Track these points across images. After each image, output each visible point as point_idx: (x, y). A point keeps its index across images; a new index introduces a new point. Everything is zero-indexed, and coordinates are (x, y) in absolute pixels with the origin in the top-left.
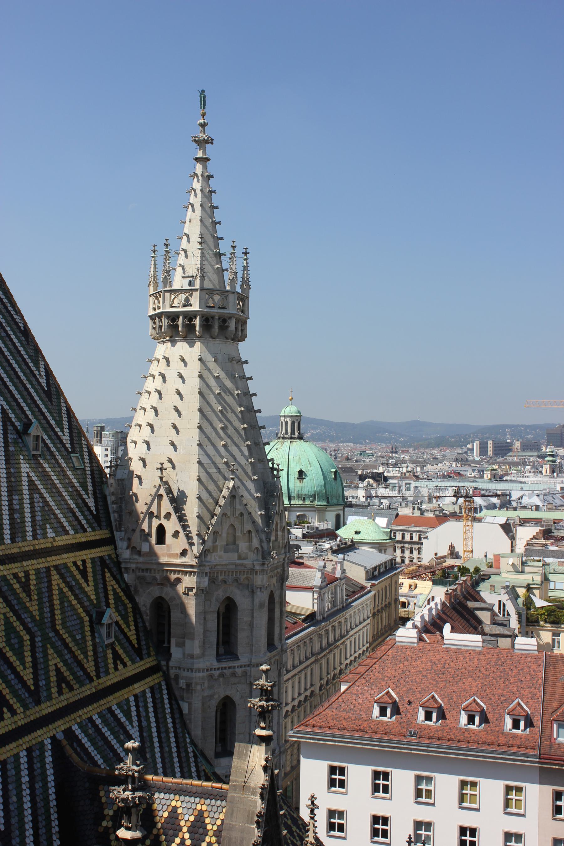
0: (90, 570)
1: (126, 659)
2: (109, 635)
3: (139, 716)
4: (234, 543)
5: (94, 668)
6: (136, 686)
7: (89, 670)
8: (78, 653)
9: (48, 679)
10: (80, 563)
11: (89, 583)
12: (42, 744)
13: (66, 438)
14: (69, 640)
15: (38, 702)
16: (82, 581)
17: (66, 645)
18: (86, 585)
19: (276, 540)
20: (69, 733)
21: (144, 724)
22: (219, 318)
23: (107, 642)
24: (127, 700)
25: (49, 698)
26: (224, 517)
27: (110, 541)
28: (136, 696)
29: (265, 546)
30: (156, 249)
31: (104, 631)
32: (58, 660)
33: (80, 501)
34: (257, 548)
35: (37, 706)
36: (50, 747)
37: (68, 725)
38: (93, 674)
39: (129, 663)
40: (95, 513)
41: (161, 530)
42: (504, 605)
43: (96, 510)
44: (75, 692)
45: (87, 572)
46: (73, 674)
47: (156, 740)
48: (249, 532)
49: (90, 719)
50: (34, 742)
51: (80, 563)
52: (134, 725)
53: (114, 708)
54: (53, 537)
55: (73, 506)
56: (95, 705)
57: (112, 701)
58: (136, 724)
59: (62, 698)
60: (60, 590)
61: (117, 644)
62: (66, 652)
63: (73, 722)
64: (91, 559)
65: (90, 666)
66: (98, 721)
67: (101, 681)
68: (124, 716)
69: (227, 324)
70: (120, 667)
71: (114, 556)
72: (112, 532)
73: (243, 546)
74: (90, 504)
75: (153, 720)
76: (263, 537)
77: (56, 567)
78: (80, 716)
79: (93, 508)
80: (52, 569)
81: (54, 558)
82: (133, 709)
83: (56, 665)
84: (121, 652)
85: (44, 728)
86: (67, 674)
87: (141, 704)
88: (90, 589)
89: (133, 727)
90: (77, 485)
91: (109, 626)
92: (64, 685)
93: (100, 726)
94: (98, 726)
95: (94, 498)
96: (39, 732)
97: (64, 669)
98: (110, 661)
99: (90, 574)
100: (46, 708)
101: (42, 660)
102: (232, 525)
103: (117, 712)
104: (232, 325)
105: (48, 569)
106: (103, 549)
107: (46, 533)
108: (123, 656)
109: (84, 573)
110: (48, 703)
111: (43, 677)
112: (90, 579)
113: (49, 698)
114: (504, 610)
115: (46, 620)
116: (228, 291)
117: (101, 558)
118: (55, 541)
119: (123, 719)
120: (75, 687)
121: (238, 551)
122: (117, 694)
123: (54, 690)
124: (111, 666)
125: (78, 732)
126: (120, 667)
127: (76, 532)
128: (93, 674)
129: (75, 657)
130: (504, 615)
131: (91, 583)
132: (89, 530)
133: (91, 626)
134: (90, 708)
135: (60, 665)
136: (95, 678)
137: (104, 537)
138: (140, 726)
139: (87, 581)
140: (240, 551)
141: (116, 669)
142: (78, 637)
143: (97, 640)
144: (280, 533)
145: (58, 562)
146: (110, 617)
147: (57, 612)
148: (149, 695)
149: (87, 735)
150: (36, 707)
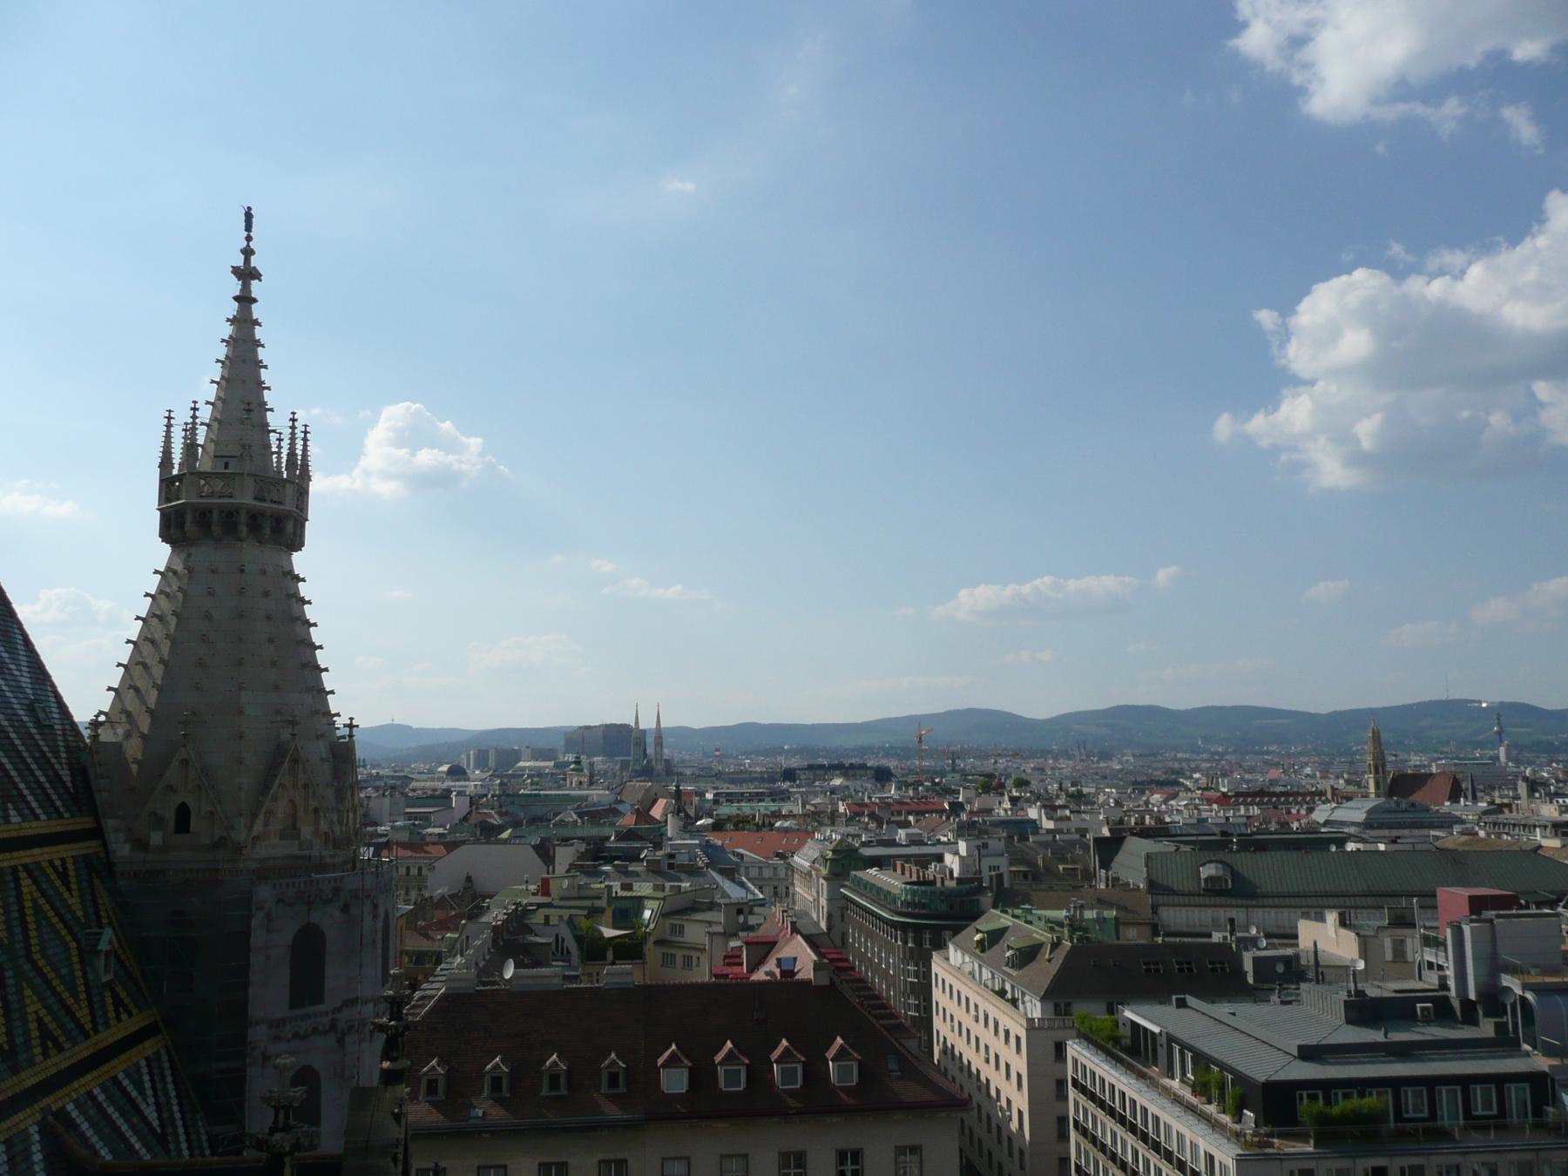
0: (72, 873)
1: (131, 1006)
2: (107, 971)
3: (154, 1088)
4: (294, 827)
5: (89, 1018)
6: (147, 1044)
7: (82, 1021)
8: (66, 995)
9: (27, 1033)
10: (58, 863)
11: (73, 892)
12: (24, 1136)
13: (25, 680)
14: (51, 976)
15: (15, 1070)
16: (63, 889)
17: (47, 982)
18: (69, 895)
19: (347, 824)
20: (61, 1114)
21: (162, 1100)
22: (272, 516)
23: (104, 979)
24: (137, 1065)
25: (31, 1063)
26: (280, 790)
27: (97, 833)
28: (148, 1059)
29: (337, 829)
30: (172, 416)
31: (101, 963)
32: (39, 1006)
33: (50, 773)
34: (326, 834)
35: (15, 1075)
36: (37, 1137)
37: (60, 1104)
38: (88, 1027)
39: (135, 1011)
40: (72, 791)
41: (183, 814)
42: (563, 940)
43: (73, 787)
44: (67, 1054)
45: (68, 876)
46: (61, 1026)
47: (179, 1123)
48: (316, 811)
49: (90, 1095)
50: (14, 1130)
51: (58, 863)
52: (150, 1102)
53: (121, 1076)
54: (19, 823)
55: (42, 779)
56: (95, 1073)
57: (118, 1067)
58: (151, 1100)
59: (49, 1062)
60: (34, 900)
61: (117, 983)
62: (49, 993)
63: (67, 1099)
64: (72, 857)
65: (83, 1013)
66: (101, 1098)
67: (100, 1036)
68: (135, 1088)
69: (281, 525)
70: (124, 1016)
71: (102, 855)
72: (97, 820)
73: (306, 831)
74: (65, 778)
75: (173, 1094)
76: (335, 817)
77: (25, 866)
78: (76, 1090)
79: (69, 784)
80: (20, 868)
81: (22, 853)
82: (146, 1078)
83: (36, 1012)
84: (123, 994)
85: (27, 1110)
86: (52, 1026)
87: (155, 1071)
88: (74, 901)
89: (148, 1105)
90: (45, 749)
91: (108, 953)
92: (50, 1044)
93: (105, 1105)
94: (100, 1103)
95: (70, 769)
96: (21, 1116)
97: (47, 1019)
98: (111, 1008)
99: (73, 880)
100: (29, 1079)
101: (16, 1006)
102: (292, 801)
103: (126, 1082)
104: (290, 527)
105: (14, 869)
106: (88, 844)
107: (9, 816)
108: (127, 1001)
109: (64, 877)
110: (30, 1071)
111: (20, 1031)
112: (74, 886)
113: (31, 1063)
114: (563, 949)
115: (18, 946)
116: (285, 480)
117: (86, 857)
118: (21, 829)
119: (134, 1094)
120: (66, 1046)
121: (298, 837)
122: (123, 1057)
123: (37, 1050)
124: (112, 1014)
125: (75, 1114)
126: (124, 1016)
127: (49, 818)
128: (88, 1027)
129: (62, 1001)
130: (562, 953)
131: (75, 893)
132: (67, 815)
133: (80, 955)
134: (89, 1077)
135: (43, 1012)
136: (91, 1033)
137: (87, 826)
138: (157, 1104)
139: (69, 890)
140: (302, 838)
141: (119, 1020)
142: (64, 971)
143: (91, 977)
144: (351, 815)
145: (27, 861)
146: (110, 942)
147: (33, 934)
148: (165, 1058)
149: (88, 1119)
150: (14, 1077)
